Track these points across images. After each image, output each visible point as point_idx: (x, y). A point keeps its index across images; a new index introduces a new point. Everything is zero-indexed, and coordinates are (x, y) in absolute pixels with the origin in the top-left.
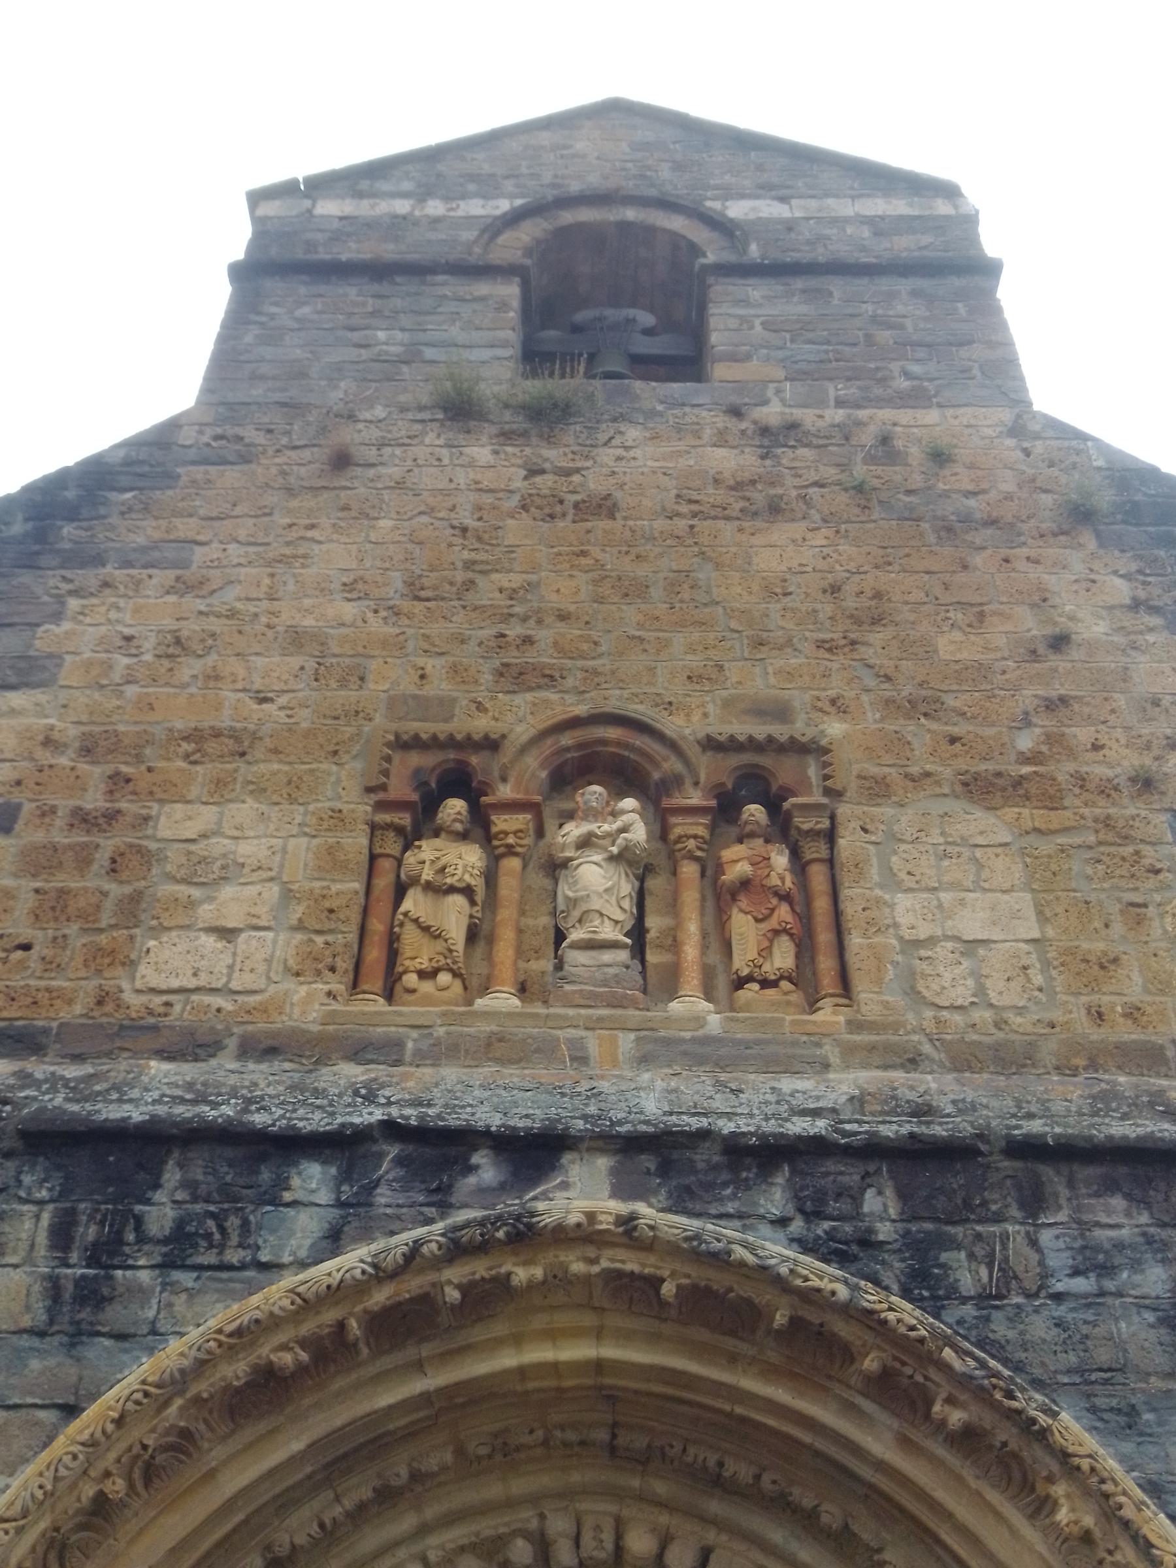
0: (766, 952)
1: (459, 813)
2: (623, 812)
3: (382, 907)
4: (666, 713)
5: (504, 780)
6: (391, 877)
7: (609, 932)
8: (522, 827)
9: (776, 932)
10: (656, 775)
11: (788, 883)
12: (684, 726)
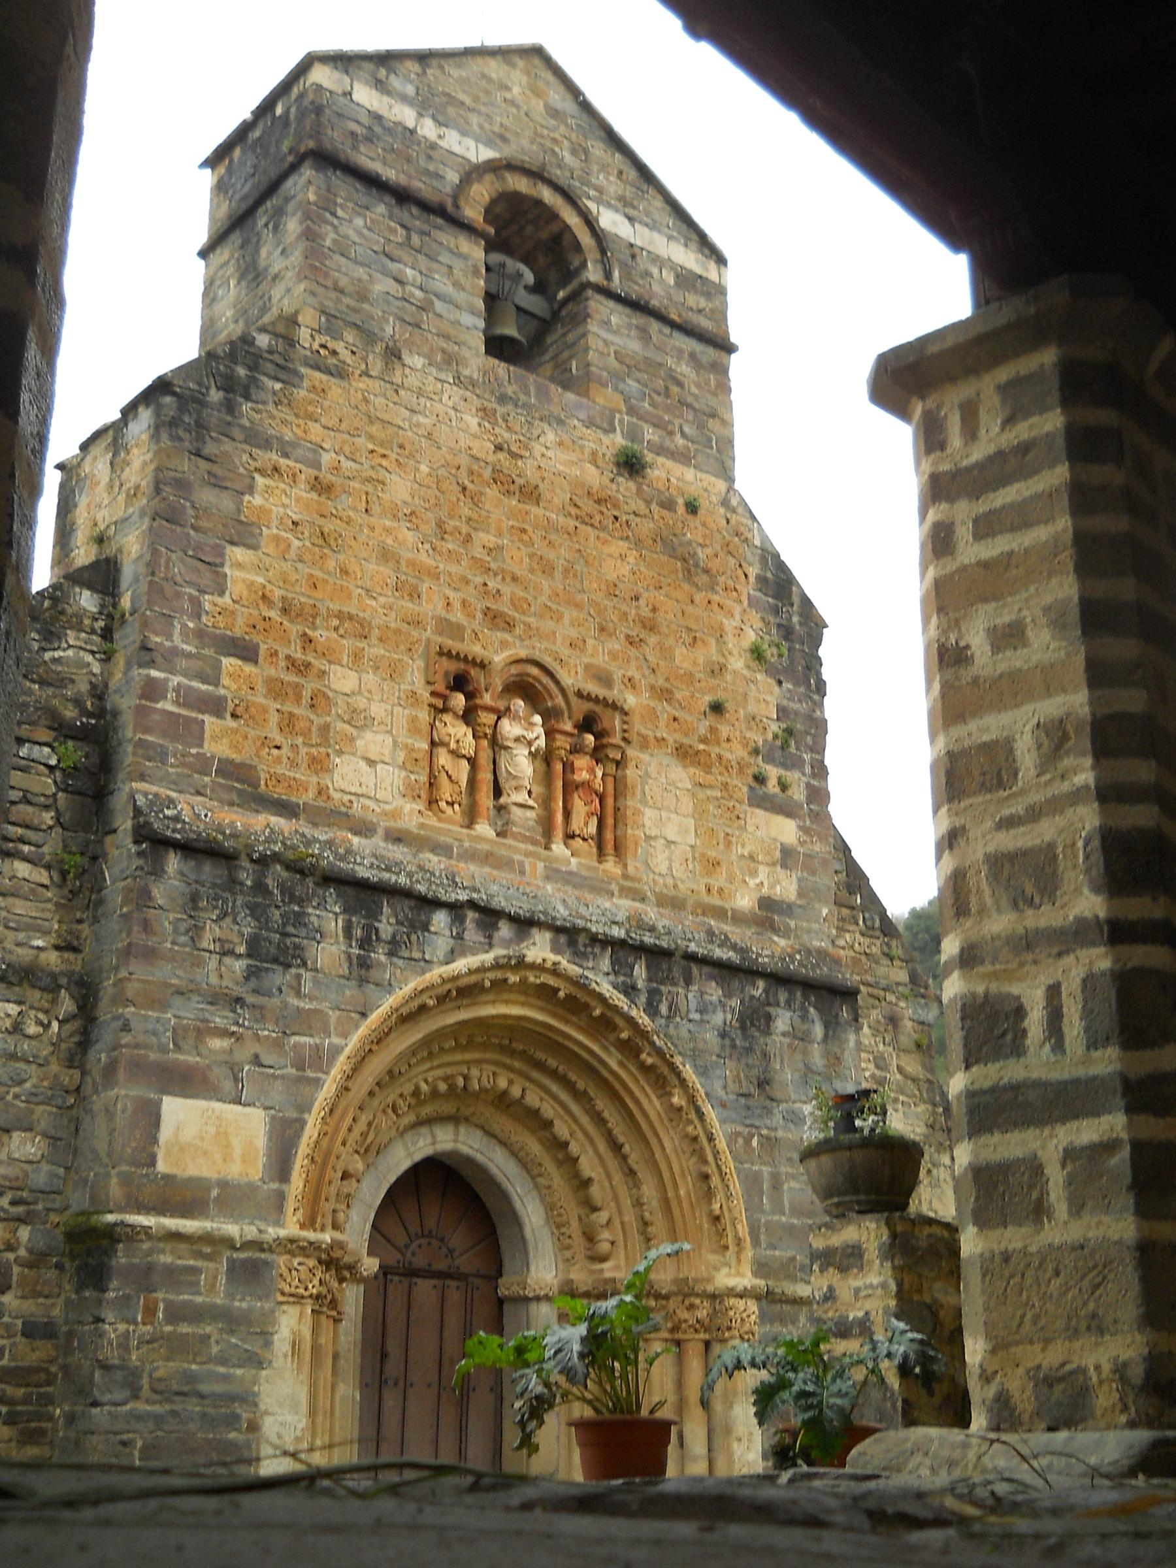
12: (567, 680)
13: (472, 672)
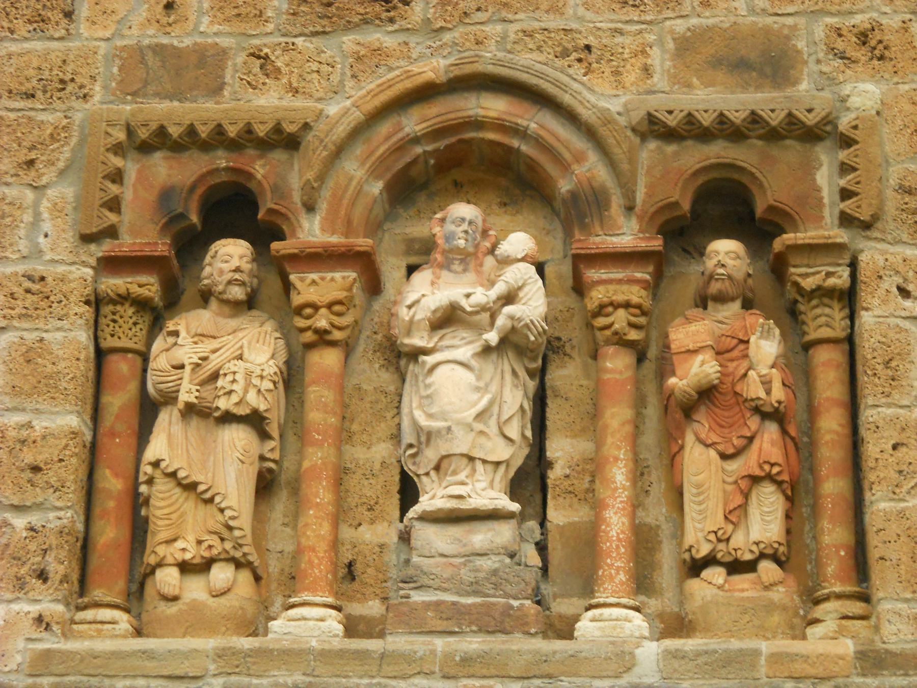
0: (736, 514)
1: (237, 270)
2: (506, 261)
3: (117, 448)
4: (578, 70)
5: (310, 208)
6: (133, 387)
7: (487, 492)
8: (341, 295)
9: (755, 480)
10: (564, 186)
11: (778, 393)
12: (605, 98)
13: (259, 169)
